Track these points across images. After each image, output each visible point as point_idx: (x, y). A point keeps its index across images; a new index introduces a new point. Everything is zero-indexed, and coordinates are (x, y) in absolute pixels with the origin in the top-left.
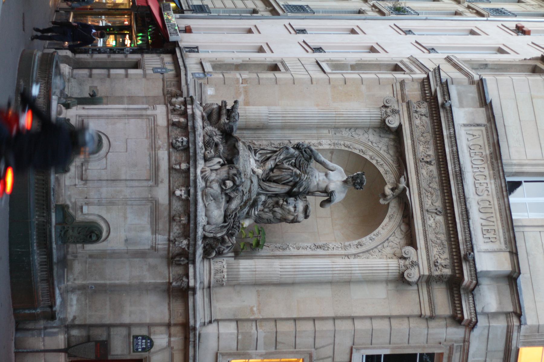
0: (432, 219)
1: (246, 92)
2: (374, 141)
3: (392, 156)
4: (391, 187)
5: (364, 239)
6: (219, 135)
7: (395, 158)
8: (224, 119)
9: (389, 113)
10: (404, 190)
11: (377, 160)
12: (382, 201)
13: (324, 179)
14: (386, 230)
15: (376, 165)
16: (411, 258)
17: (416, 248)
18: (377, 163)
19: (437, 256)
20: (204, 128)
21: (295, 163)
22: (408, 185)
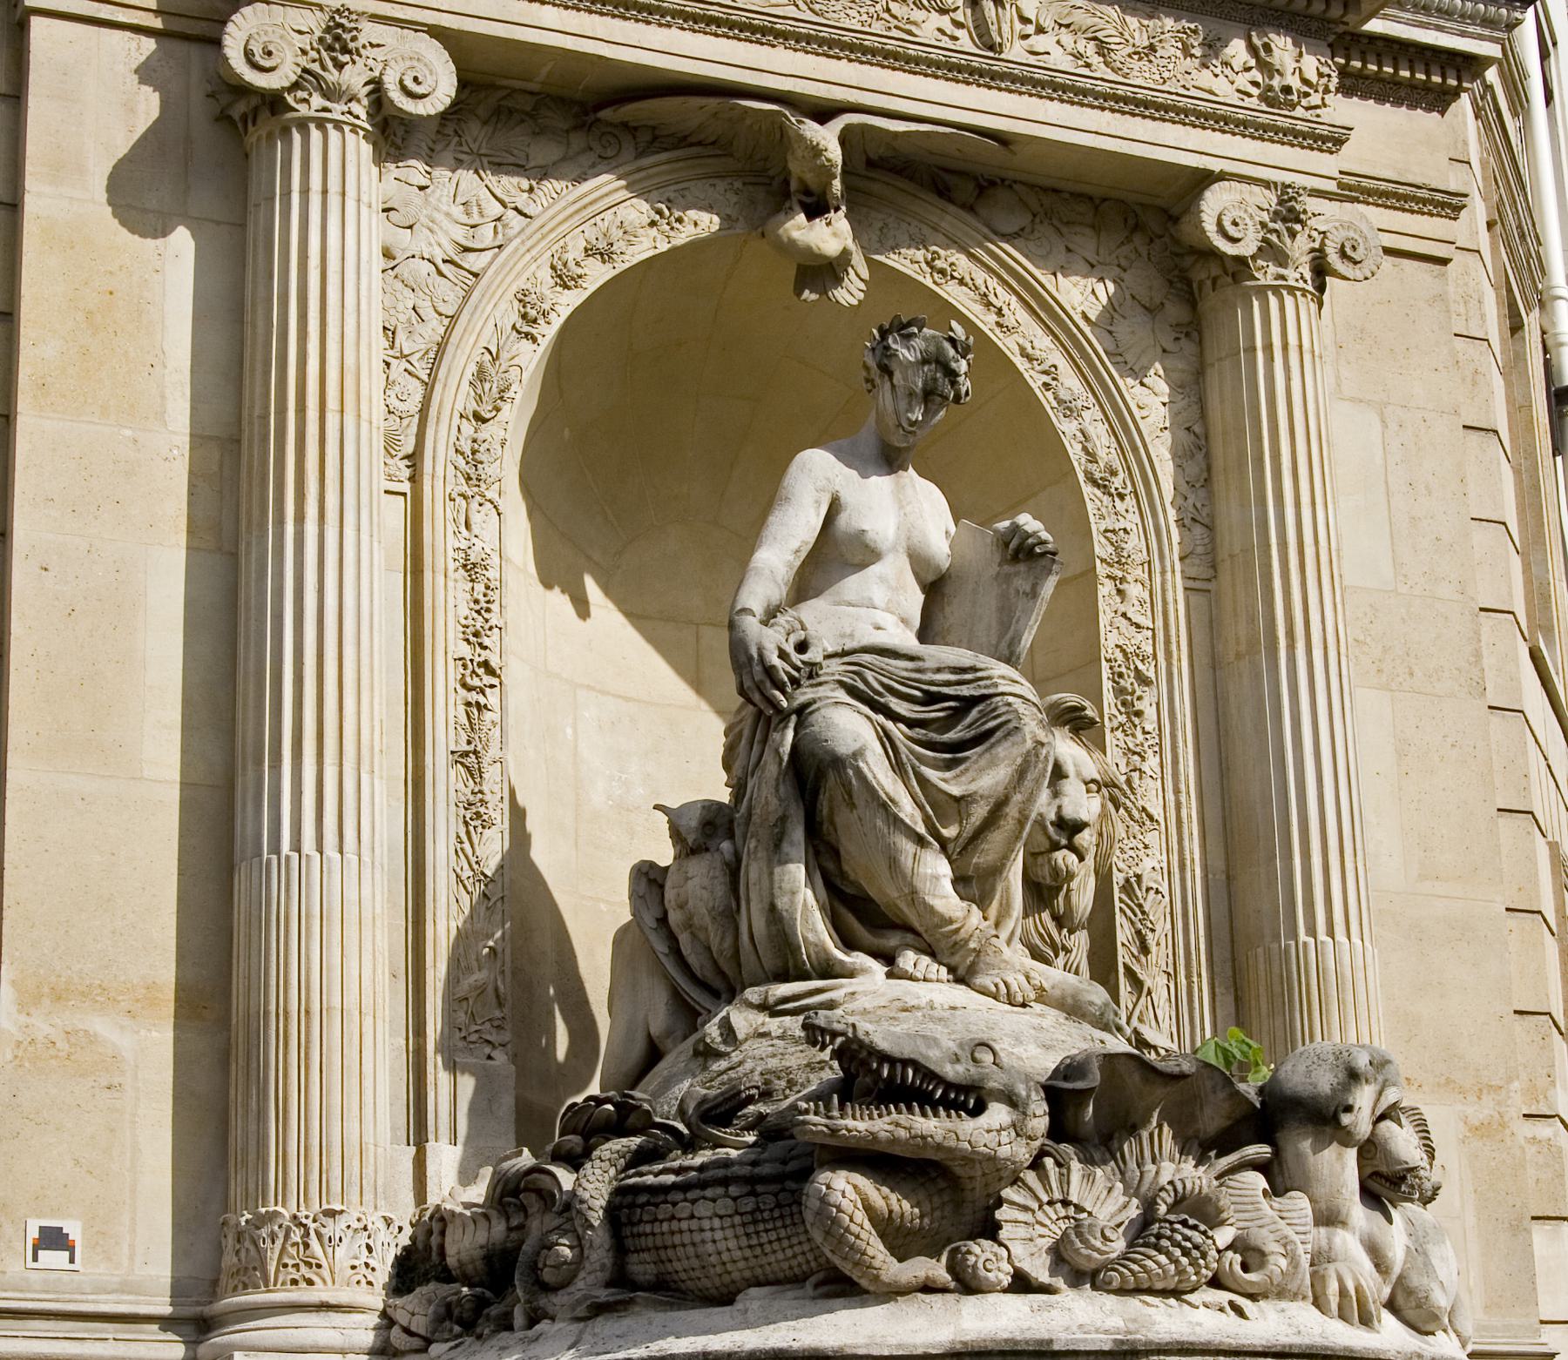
0: (1039, 43)
1: (58, 997)
2: (460, 234)
3: (564, 159)
4: (801, 217)
5: (1075, 451)
6: (1065, 1180)
7: (578, 140)
8: (989, 1131)
9: (354, 77)
10: (844, 139)
11: (589, 252)
12: (850, 292)
13: (882, 579)
14: (1022, 315)
15: (621, 267)
16: (1265, 217)
17: (1205, 179)
18: (606, 256)
19: (1243, 81)
20: (1022, 1284)
21: (911, 723)
22: (823, 112)
